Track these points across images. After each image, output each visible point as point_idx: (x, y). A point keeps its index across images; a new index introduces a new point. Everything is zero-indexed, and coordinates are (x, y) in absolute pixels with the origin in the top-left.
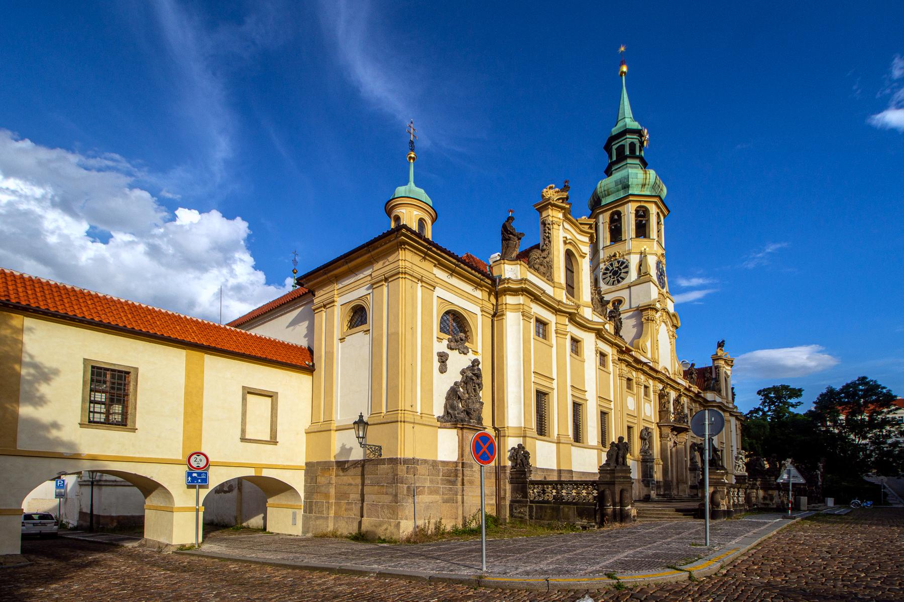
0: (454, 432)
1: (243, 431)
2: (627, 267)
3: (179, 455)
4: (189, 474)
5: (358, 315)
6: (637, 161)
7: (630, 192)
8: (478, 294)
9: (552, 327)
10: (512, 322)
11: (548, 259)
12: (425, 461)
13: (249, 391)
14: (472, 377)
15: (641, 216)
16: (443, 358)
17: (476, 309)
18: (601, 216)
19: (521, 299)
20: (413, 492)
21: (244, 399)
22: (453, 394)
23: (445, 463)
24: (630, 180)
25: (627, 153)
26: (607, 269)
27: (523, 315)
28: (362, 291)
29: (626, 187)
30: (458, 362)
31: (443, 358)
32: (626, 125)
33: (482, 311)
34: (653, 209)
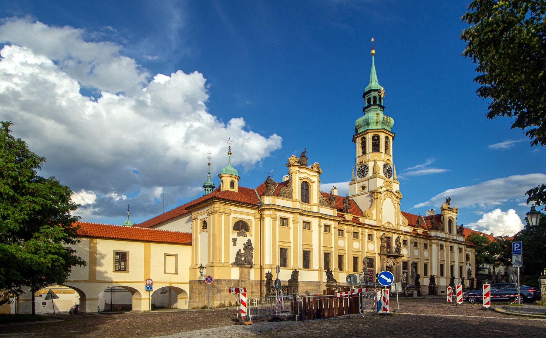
1: (165, 270)
2: (367, 168)
3: (143, 280)
4: (146, 286)
5: (205, 225)
6: (377, 107)
7: (370, 128)
8: (253, 211)
12: (225, 280)
13: (166, 255)
14: (248, 246)
15: (376, 140)
17: (252, 218)
18: (357, 139)
21: (165, 258)
22: (239, 254)
23: (234, 280)
24: (370, 120)
25: (372, 103)
26: (359, 169)
28: (205, 216)
29: (368, 124)
30: (242, 241)
32: (371, 87)
34: (382, 136)
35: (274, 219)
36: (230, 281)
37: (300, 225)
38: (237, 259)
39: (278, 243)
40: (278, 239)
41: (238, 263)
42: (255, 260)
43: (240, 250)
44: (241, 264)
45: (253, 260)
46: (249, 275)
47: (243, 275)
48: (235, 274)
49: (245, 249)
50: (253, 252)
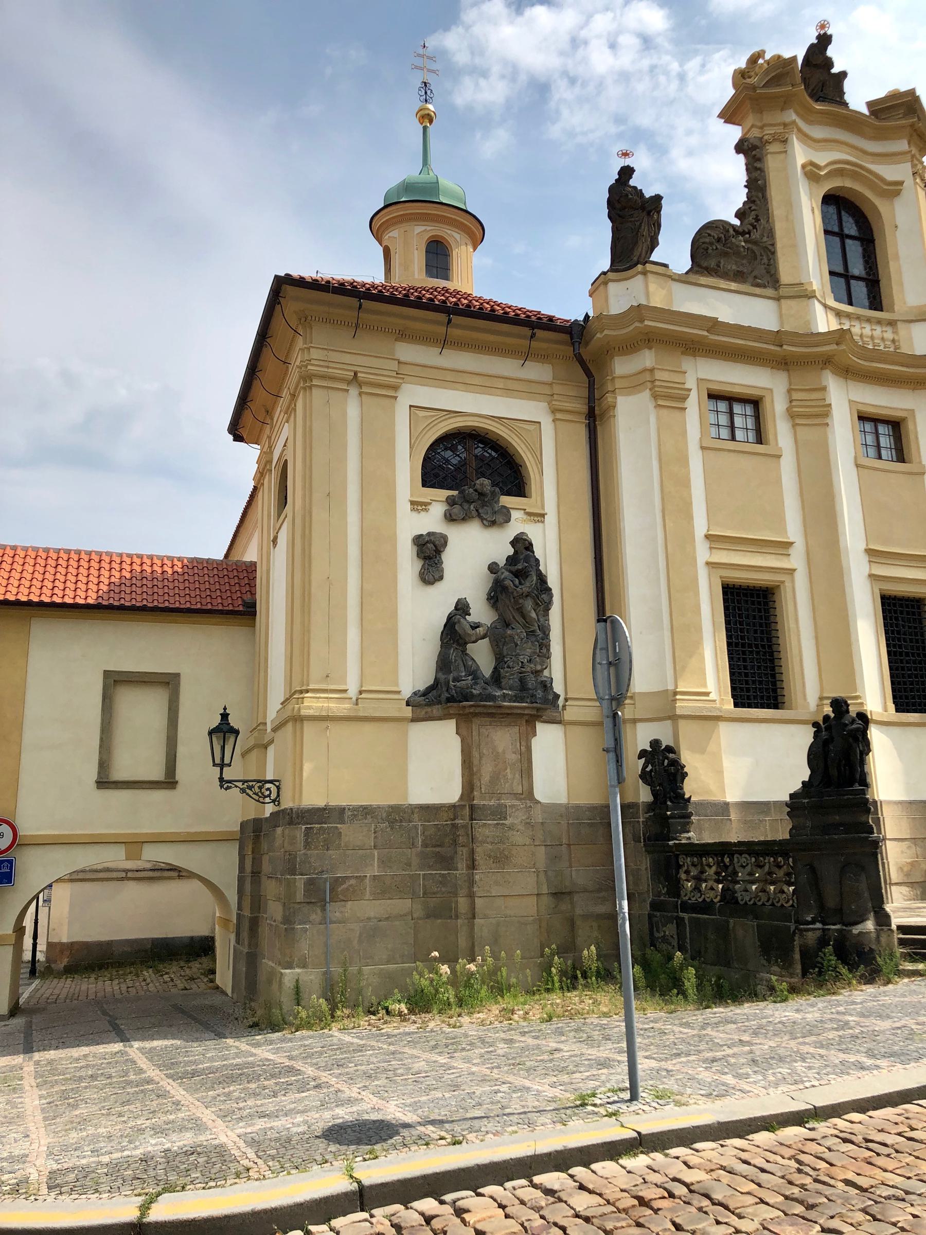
0: (451, 724)
9: (777, 406)
10: (633, 421)
11: (755, 235)
12: (366, 811)
14: (518, 582)
16: (430, 552)
19: (647, 359)
20: (322, 894)
22: (454, 633)
27: (655, 397)
30: (473, 553)
31: (430, 552)
33: (554, 411)
35: (671, 398)
36: (398, 816)
37: (843, 436)
38: (443, 664)
39: (703, 553)
40: (700, 527)
41: (452, 693)
42: (567, 663)
43: (462, 608)
44: (467, 697)
45: (556, 671)
46: (527, 771)
47: (486, 771)
48: (432, 767)
49: (498, 594)
50: (555, 614)
